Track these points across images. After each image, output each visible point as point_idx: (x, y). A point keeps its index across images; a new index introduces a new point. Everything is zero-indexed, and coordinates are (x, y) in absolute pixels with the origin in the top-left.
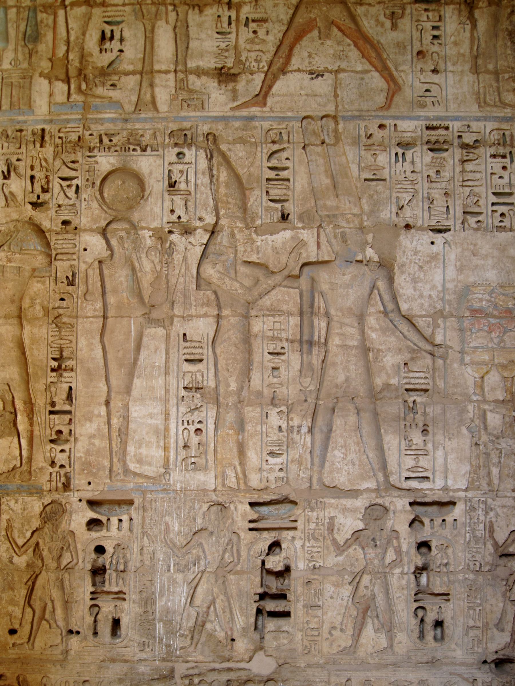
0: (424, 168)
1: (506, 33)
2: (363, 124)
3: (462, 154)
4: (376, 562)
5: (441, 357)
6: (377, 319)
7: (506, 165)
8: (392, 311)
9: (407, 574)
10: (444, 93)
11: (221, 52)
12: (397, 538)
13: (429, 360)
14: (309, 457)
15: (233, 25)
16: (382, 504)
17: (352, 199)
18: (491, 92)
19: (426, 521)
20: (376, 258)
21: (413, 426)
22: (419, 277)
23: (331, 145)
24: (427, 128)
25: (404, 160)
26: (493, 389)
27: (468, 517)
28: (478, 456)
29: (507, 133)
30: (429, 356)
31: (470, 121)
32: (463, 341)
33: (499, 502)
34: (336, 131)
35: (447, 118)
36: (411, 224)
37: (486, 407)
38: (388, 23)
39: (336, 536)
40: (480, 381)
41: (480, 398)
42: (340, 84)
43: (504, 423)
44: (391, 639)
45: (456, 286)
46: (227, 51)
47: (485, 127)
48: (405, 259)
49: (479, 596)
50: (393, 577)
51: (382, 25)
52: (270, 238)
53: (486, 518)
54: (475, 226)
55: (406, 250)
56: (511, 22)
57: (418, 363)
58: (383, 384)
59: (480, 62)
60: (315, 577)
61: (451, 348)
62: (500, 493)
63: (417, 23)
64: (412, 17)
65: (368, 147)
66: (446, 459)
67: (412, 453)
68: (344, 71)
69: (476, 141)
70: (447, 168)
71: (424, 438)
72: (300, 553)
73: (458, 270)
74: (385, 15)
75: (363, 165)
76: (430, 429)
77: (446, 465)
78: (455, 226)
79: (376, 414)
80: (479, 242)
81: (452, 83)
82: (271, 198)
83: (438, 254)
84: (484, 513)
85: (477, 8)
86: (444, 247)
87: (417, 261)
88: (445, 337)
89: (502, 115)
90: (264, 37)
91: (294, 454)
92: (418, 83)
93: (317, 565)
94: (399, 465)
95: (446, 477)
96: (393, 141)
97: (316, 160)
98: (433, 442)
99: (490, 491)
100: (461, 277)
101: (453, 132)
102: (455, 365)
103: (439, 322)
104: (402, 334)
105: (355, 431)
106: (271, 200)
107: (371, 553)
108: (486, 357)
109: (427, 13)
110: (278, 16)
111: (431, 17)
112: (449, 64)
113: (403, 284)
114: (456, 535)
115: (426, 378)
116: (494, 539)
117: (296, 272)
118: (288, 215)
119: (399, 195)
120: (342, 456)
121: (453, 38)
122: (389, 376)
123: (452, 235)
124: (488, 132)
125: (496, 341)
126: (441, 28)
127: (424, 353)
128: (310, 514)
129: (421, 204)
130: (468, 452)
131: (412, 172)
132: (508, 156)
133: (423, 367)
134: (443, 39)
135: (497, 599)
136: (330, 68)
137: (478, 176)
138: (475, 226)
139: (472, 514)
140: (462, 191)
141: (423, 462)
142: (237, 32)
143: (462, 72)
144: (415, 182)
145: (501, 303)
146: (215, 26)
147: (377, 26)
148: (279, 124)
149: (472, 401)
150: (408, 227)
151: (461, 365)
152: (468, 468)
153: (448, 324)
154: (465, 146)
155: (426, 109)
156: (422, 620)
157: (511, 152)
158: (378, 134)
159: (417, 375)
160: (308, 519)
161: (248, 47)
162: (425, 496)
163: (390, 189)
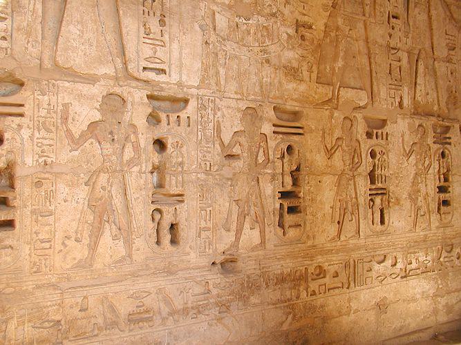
9: (145, 172)
14: (39, 27)
19: (163, 116)
33: (225, 103)
37: (215, 8)
39: (71, 126)
43: (230, 27)
44: (129, 243)
50: (131, 176)
60: (47, 176)
66: (181, 53)
72: (28, 145)
77: (180, 59)
91: (23, 20)
93: (49, 161)
105: (93, 7)
107: (108, 148)
120: (78, 33)
128: (40, 97)
130: (199, 50)
139: (203, 112)
141: (160, 53)
160: (38, 105)
162: (162, 89)
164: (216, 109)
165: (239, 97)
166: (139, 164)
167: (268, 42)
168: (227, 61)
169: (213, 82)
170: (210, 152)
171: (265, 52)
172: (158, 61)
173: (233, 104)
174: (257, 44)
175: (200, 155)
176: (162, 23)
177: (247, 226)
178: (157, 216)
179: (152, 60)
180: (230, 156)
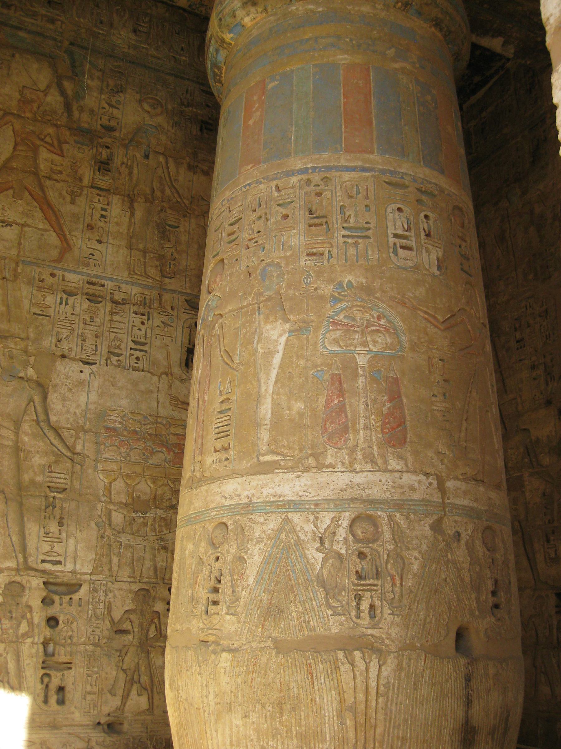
0: (81, 312)
1: (155, 224)
2: (38, 270)
3: (112, 308)
4: (11, 631)
6: (30, 426)
7: (144, 321)
8: (43, 421)
9: (37, 644)
10: (104, 259)
12: (31, 612)
13: (69, 464)
16: (20, 581)
18: (139, 265)
19: (56, 598)
20: (35, 377)
21: (52, 517)
23: (11, 281)
24: (88, 283)
25: (67, 304)
26: (118, 493)
27: (91, 597)
28: (102, 547)
29: (147, 297)
30: (70, 461)
31: (121, 283)
32: (98, 452)
33: (117, 585)
34: (15, 270)
36: (66, 354)
38: (68, 198)
40: (108, 485)
41: (107, 499)
42: (24, 235)
43: (125, 521)
45: (96, 408)
47: (132, 290)
48: (58, 381)
49: (97, 665)
50: (25, 646)
51: (64, 198)
53: (105, 598)
54: (116, 363)
55: (60, 374)
56: (160, 217)
57: (61, 465)
58: (30, 480)
59: (134, 241)
61: (88, 457)
62: (118, 579)
63: (90, 203)
64: (87, 197)
65: (40, 289)
67: (48, 539)
68: (28, 226)
69: (123, 299)
70: (99, 315)
71: (60, 528)
73: (99, 396)
74: (67, 190)
75: (34, 301)
76: (65, 521)
77: (75, 552)
79: (21, 505)
80: (118, 376)
83: (85, 381)
84: (104, 594)
85: (136, 201)
87: (67, 384)
88: (84, 446)
92: (85, 247)
94: (37, 549)
95: (75, 562)
96: (60, 287)
98: (67, 532)
99: (110, 576)
100: (101, 402)
101: (107, 289)
102: (90, 471)
103: (80, 435)
104: (50, 440)
108: (114, 467)
109: (99, 197)
111: (101, 201)
112: (110, 238)
113: (54, 401)
114: (80, 612)
115: (65, 479)
116: (111, 617)
121: (116, 219)
122: (35, 474)
123: (97, 368)
124: (133, 293)
125: (123, 455)
126: (108, 210)
127: (66, 458)
129: (76, 339)
130: (94, 542)
131: (72, 314)
132: (147, 315)
133: (64, 469)
134: (109, 219)
135: (111, 668)
136: (18, 221)
137: (122, 326)
138: (116, 363)
139: (95, 594)
140: (108, 335)
143: (119, 246)
144: (73, 322)
145: (130, 426)
147: (59, 198)
149: (101, 502)
151: (95, 471)
152: (94, 556)
153: (87, 437)
154: (114, 302)
155: (88, 268)
156: (47, 686)
157: (148, 312)
158: (50, 280)
159: (59, 475)
162: (57, 577)
163: (53, 324)
164: (107, 591)
165: (132, 580)
166: (32, 636)
167: (165, 531)
168: (122, 551)
169: (106, 569)
170: (99, 628)
171: (162, 540)
172: (55, 554)
173: (126, 586)
174: (153, 534)
175: (90, 630)
176: (61, 524)
177: (134, 692)
178: (46, 680)
179: (49, 554)
180: (124, 632)
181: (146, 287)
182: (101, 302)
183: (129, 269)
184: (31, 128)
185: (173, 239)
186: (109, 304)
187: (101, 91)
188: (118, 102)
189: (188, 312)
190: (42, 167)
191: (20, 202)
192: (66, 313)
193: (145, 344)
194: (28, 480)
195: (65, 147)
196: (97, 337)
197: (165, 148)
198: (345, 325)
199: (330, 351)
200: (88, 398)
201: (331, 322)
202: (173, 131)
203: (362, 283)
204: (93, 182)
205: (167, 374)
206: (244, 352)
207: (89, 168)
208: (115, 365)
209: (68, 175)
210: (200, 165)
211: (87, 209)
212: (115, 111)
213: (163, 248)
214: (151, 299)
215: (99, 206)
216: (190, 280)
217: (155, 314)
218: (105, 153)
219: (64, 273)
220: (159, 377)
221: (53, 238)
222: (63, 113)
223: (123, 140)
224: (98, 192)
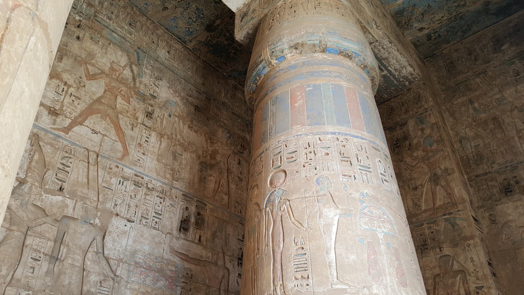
2: (109, 162)
3: (146, 191)
5: (117, 282)
6: (92, 255)
10: (145, 164)
11: (54, 101)
13: (111, 283)
15: (64, 92)
17: (95, 193)
20: (99, 225)
22: (116, 239)
25: (123, 185)
30: (112, 280)
35: (144, 174)
38: (130, 127)
42: (104, 141)
45: (131, 249)
46: (57, 101)
51: (127, 126)
52: (50, 196)
55: (114, 225)
61: (123, 279)
65: (109, 173)
68: (107, 136)
69: (153, 188)
70: (139, 195)
73: (133, 241)
75: (104, 180)
78: (137, 221)
80: (145, 232)
81: (149, 161)
82: (57, 177)
83: (127, 231)
86: (130, 229)
87: (117, 232)
88: (121, 272)
89: (164, 181)
90: (77, 105)
97: (83, 169)
100: (134, 245)
106: (56, 178)
108: (136, 287)
110: (85, 100)
112: (149, 153)
113: (108, 241)
115: (108, 291)
117: (59, 219)
118: (64, 189)
119: (117, 199)
124: (158, 186)
125: (142, 280)
127: (110, 278)
129: (125, 206)
132: (163, 199)
133: (108, 285)
137: (150, 202)
138: (145, 224)
142: (65, 96)
144: (125, 196)
145: (148, 262)
146: (55, 88)
148: (71, 145)
150: (117, 215)
151: (125, 288)
153: (124, 266)
154: (148, 188)
155: (136, 167)
158: (115, 170)
159: (104, 289)
161: (68, 105)
163: (114, 195)
181: (164, 183)
182: (140, 187)
183: (156, 172)
184: (114, 84)
185: (179, 161)
186: (145, 189)
187: (151, 76)
188: (158, 84)
189: (183, 201)
190: (118, 106)
191: (104, 122)
192: (122, 190)
193: (161, 215)
194: (86, 290)
195: (131, 99)
196: (137, 206)
197: (179, 114)
198: (369, 216)
199: (364, 228)
200: (127, 242)
201: (362, 213)
202: (183, 107)
203: (373, 195)
204: (143, 121)
205: (169, 233)
206: (311, 222)
207: (142, 114)
208: (144, 225)
209: (131, 115)
210: (194, 127)
211: (139, 135)
212: (157, 89)
213: (174, 164)
214: (166, 191)
215: (145, 135)
216: (185, 184)
217: (167, 199)
218: (150, 109)
219: (123, 167)
220: (166, 235)
221: (119, 146)
222: (131, 81)
223: (159, 104)
224: (145, 127)
